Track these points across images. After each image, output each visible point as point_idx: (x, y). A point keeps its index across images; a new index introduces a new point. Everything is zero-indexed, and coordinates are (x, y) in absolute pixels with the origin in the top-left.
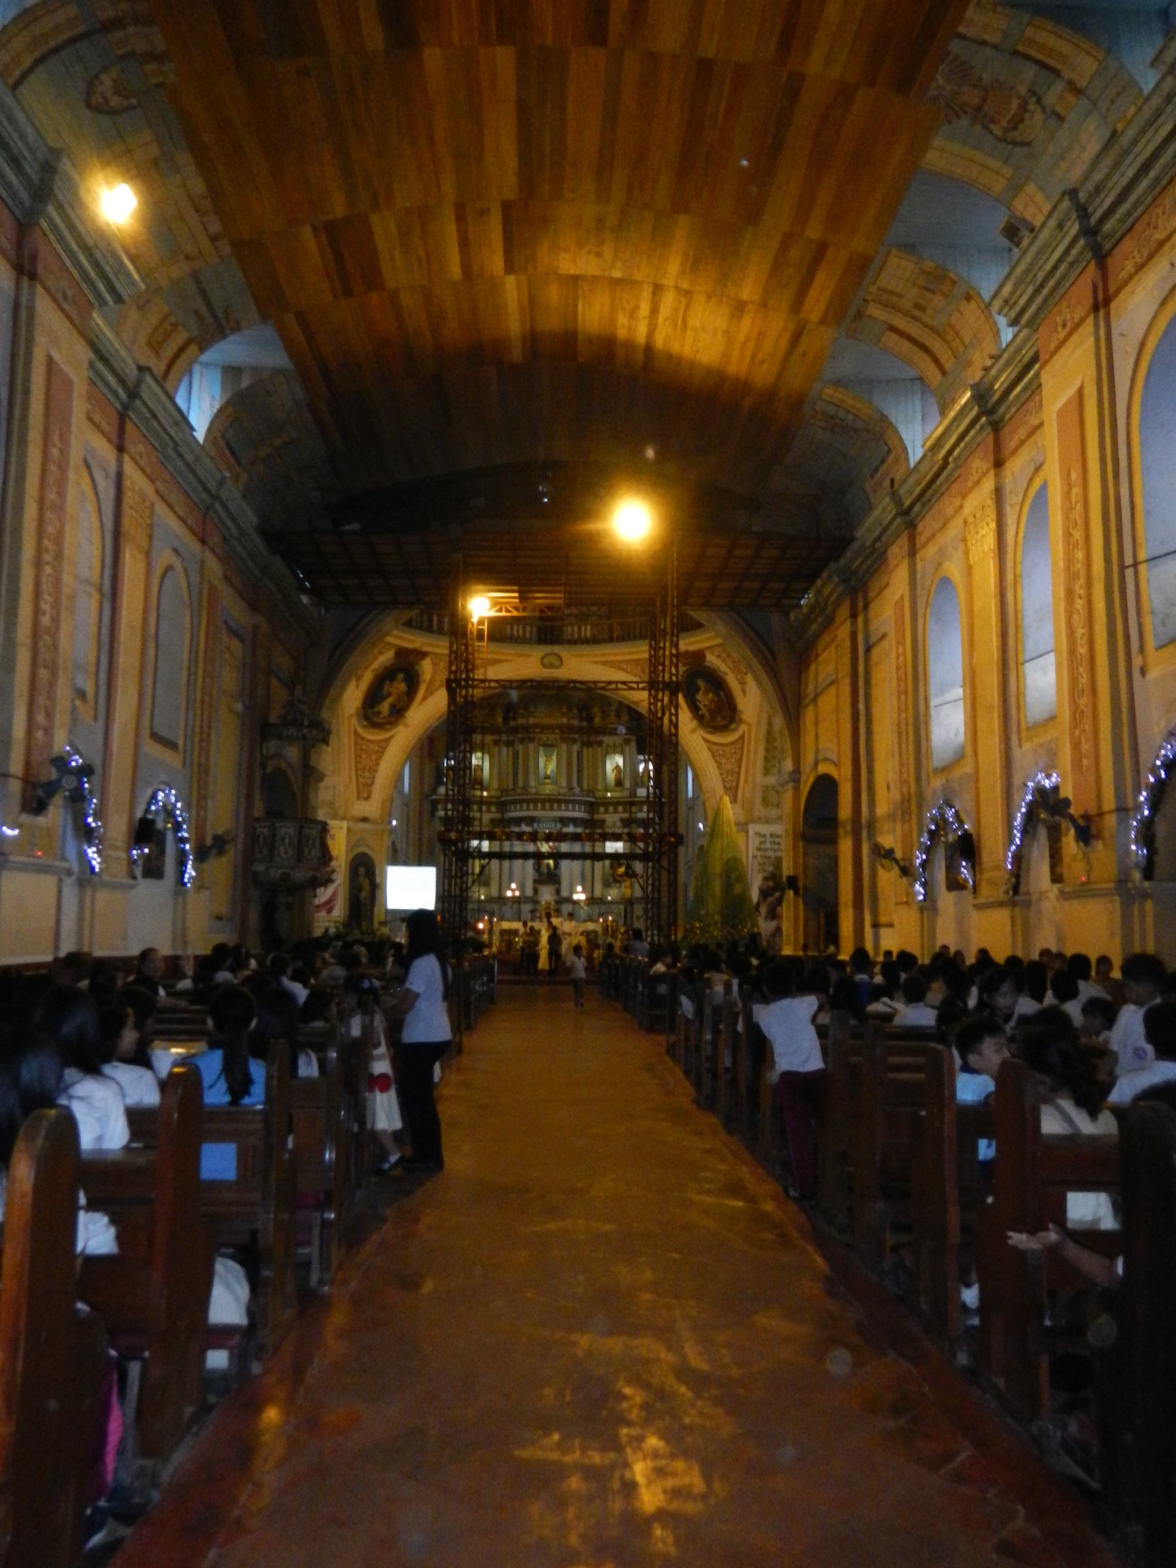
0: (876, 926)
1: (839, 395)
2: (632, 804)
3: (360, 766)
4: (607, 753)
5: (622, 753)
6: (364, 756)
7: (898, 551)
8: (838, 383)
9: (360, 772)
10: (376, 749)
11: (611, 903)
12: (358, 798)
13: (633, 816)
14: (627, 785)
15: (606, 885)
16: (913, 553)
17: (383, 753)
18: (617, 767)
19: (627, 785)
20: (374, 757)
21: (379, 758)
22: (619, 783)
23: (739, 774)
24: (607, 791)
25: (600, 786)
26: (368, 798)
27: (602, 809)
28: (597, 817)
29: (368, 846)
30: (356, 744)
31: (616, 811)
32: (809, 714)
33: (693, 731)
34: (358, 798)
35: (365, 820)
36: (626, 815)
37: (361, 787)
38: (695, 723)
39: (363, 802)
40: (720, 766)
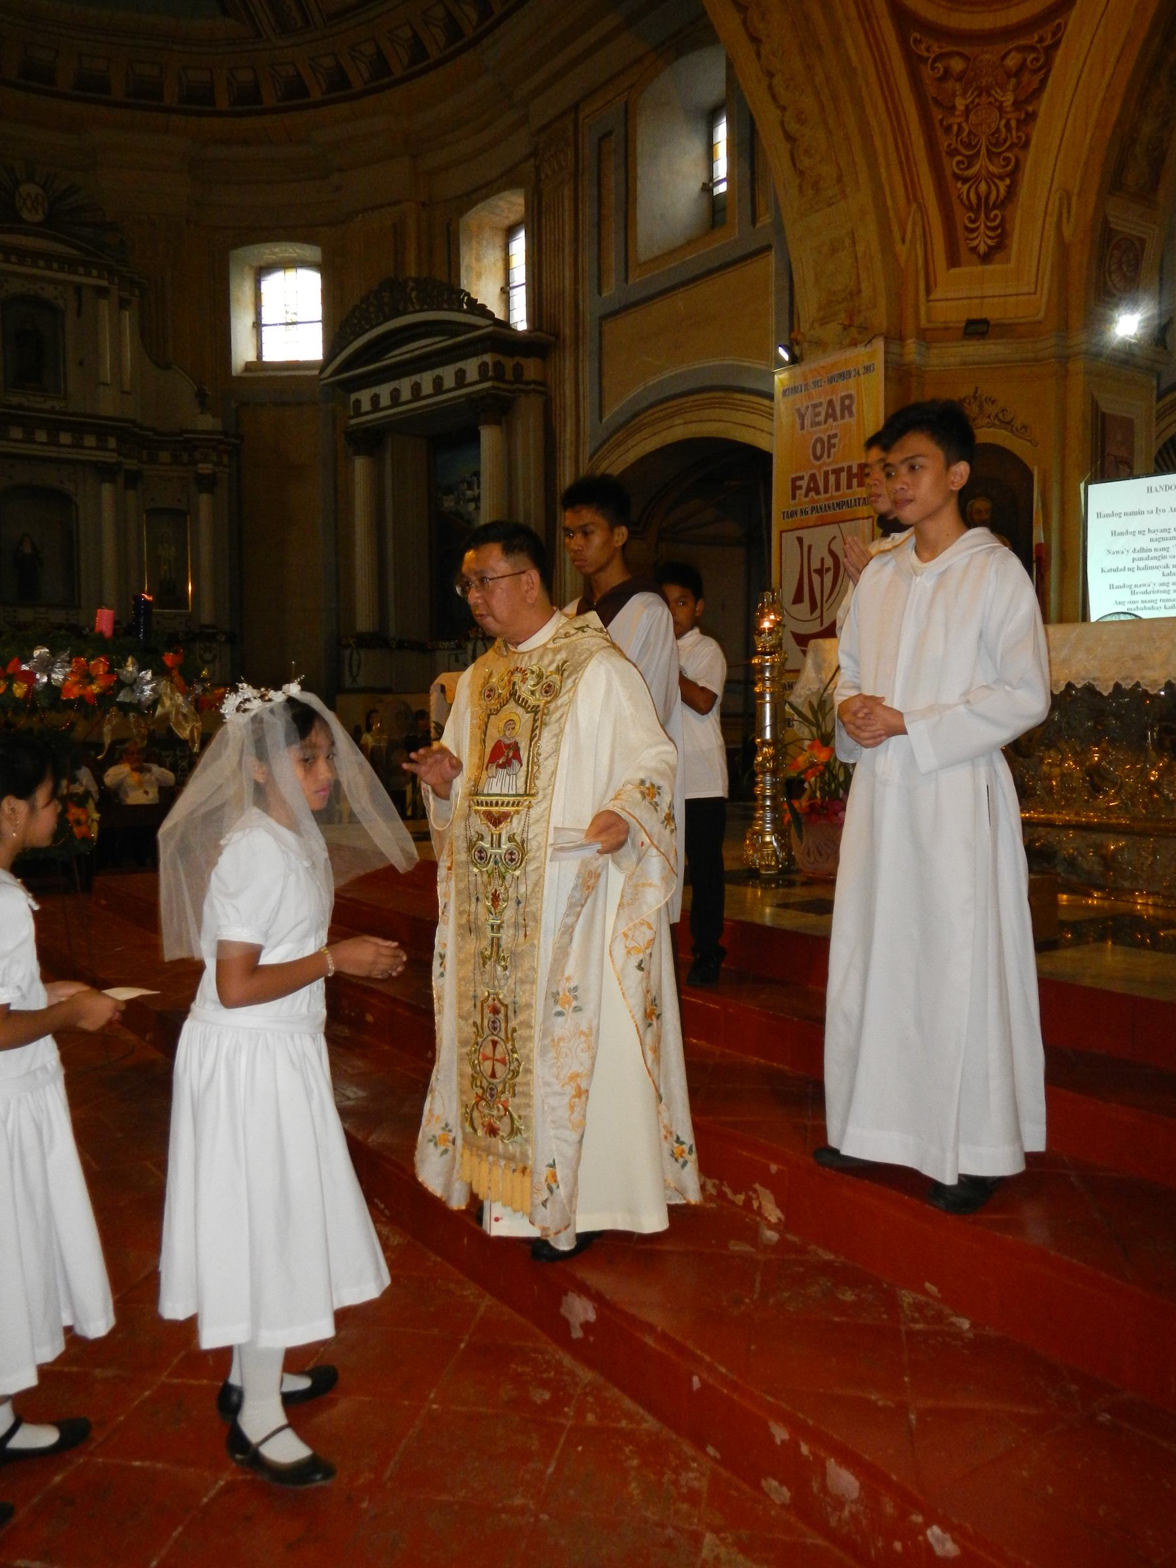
3: (944, 142)
6: (960, 104)
9: (951, 165)
10: (1012, 62)
12: (953, 261)
17: (1047, 66)
20: (1008, 99)
21: (1027, 102)
26: (998, 248)
29: (1008, 424)
30: (913, 61)
34: (953, 261)
35: (977, 329)
37: (962, 217)
39: (980, 268)
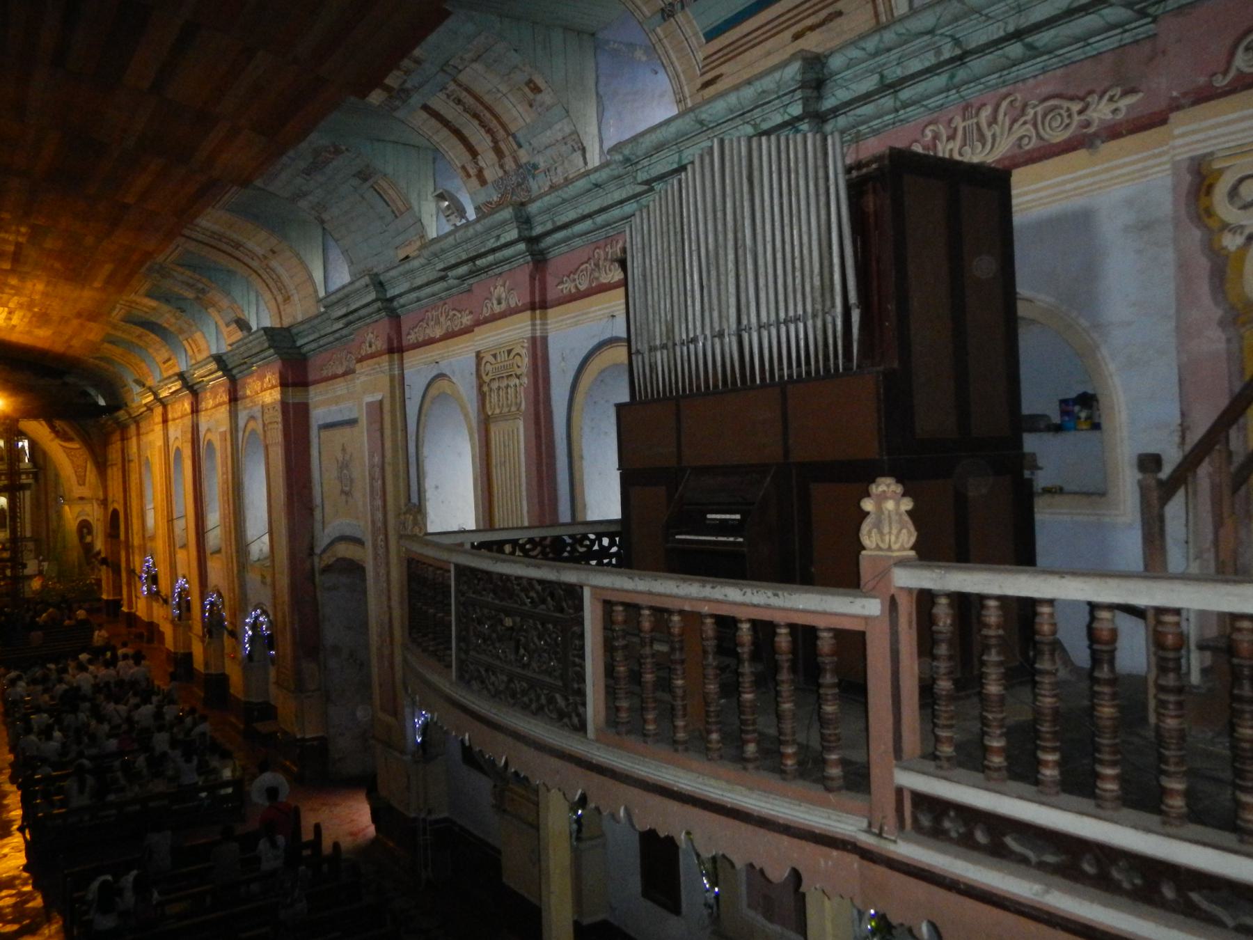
0: (136, 597)
1: (97, 362)
7: (133, 428)
8: (96, 358)
16: (138, 435)
23: (86, 467)
32: (109, 471)
33: (52, 440)
38: (53, 435)
40: (73, 462)
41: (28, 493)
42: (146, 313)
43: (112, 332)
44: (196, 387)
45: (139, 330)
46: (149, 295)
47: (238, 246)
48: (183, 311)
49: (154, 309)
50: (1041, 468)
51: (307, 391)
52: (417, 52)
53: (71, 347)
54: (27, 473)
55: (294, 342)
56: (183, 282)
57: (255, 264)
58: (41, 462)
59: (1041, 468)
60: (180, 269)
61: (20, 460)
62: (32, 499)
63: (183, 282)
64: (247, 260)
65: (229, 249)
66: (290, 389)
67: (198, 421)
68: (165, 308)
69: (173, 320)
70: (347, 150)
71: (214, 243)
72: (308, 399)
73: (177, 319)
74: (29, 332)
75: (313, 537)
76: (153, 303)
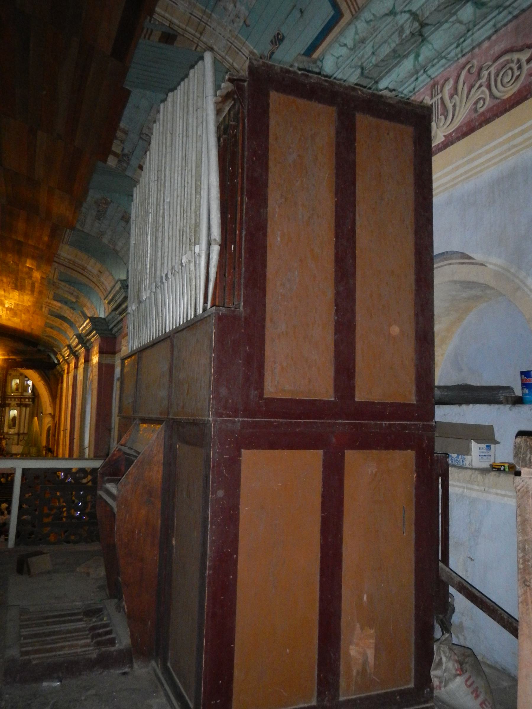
2: (21, 398)
4: (13, 378)
5: (19, 378)
8: (47, 336)
11: (11, 434)
13: (22, 402)
14: (20, 390)
15: (10, 427)
18: (17, 383)
19: (20, 390)
22: (17, 389)
24: (12, 393)
25: (9, 391)
27: (9, 400)
28: (7, 402)
31: (15, 401)
33: (39, 381)
36: (19, 402)
38: (40, 379)
41: (28, 409)
42: (58, 310)
43: (47, 321)
44: (77, 353)
45: (59, 321)
46: (55, 299)
47: (84, 269)
48: (74, 309)
49: (61, 308)
50: (498, 443)
51: (114, 357)
52: (122, 125)
53: (32, 329)
54: (29, 398)
55: (108, 326)
56: (67, 291)
57: (94, 280)
58: (37, 394)
59: (498, 443)
60: (63, 284)
61: (27, 391)
62: (30, 412)
63: (67, 291)
64: (91, 278)
65: (81, 271)
66: (104, 355)
67: (77, 373)
68: (65, 308)
69: (71, 315)
70: (111, 201)
71: (71, 266)
72: (114, 362)
73: (73, 314)
74: (9, 319)
75: (109, 447)
76: (59, 304)
